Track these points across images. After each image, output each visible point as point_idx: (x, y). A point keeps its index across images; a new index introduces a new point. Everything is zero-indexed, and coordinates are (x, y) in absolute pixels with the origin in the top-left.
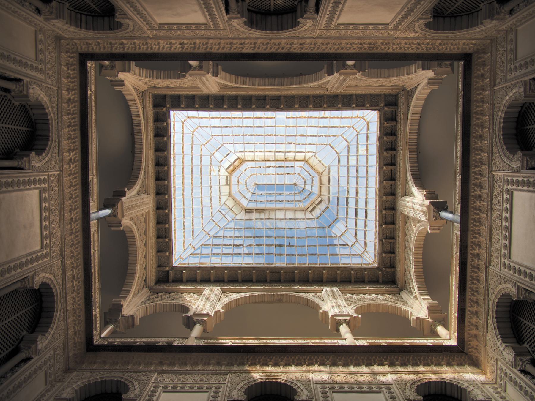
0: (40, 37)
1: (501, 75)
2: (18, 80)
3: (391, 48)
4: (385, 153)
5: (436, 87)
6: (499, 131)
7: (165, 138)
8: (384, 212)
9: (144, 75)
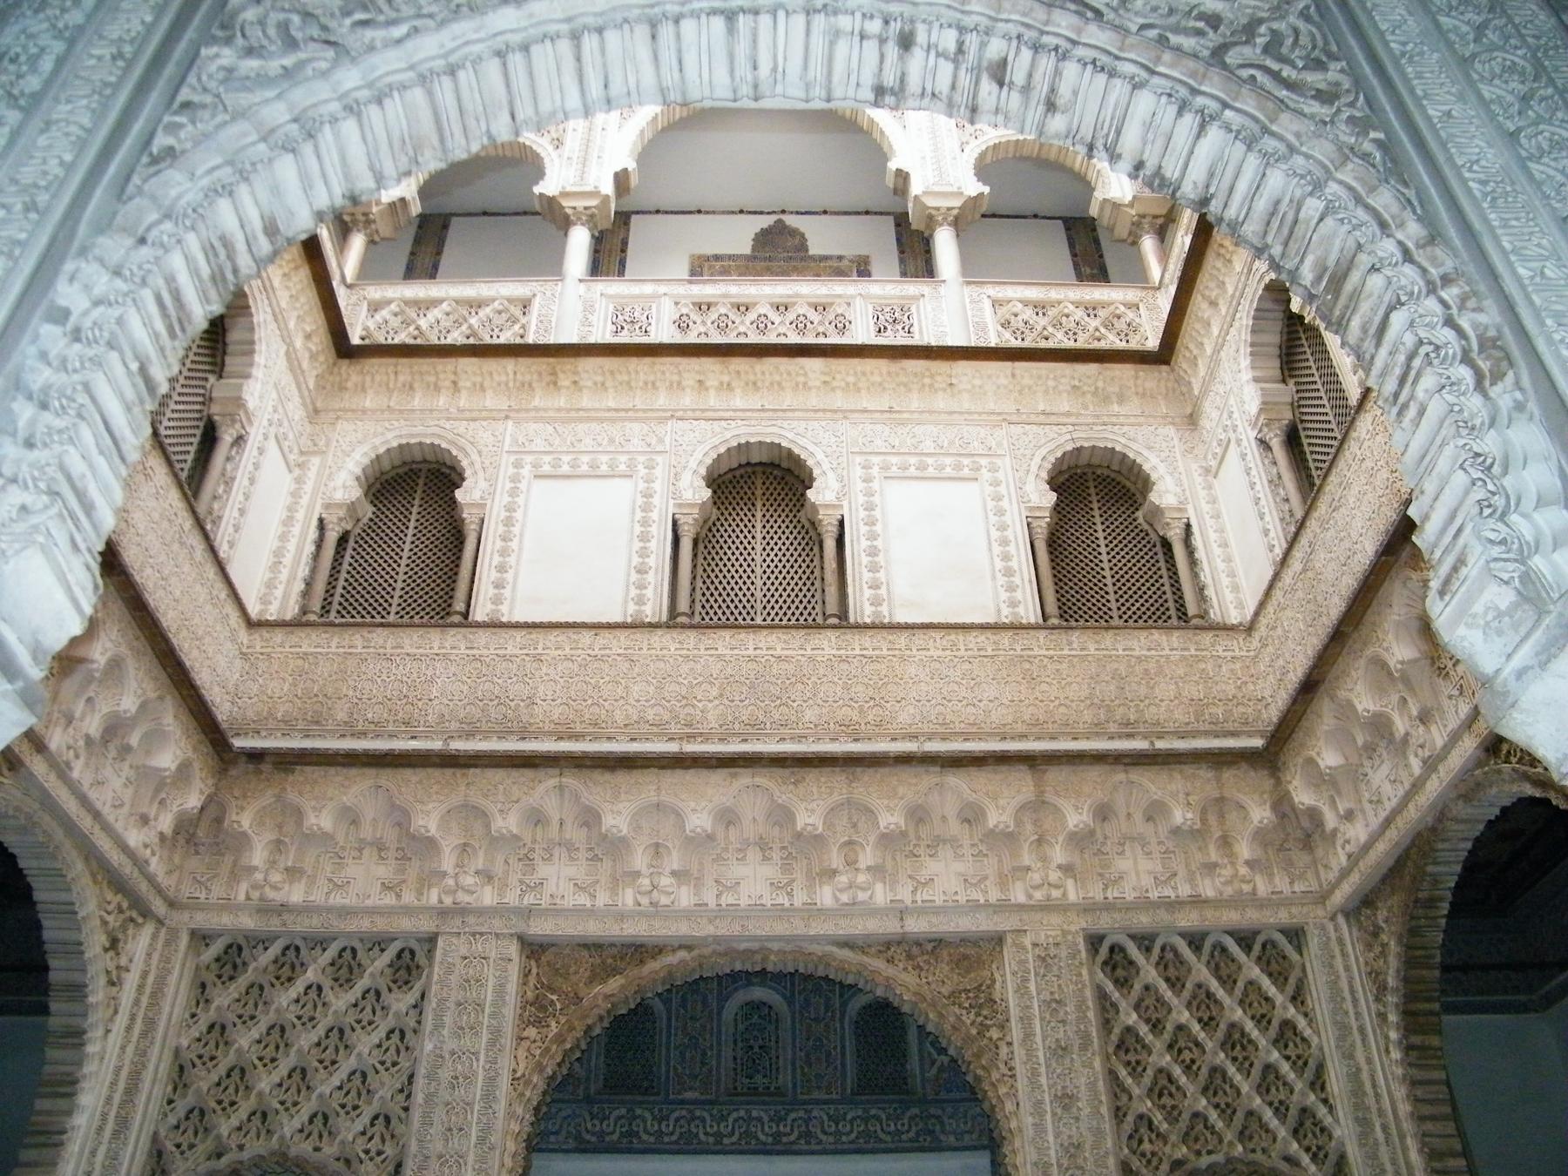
0: (1214, 463)
2: (1264, 444)
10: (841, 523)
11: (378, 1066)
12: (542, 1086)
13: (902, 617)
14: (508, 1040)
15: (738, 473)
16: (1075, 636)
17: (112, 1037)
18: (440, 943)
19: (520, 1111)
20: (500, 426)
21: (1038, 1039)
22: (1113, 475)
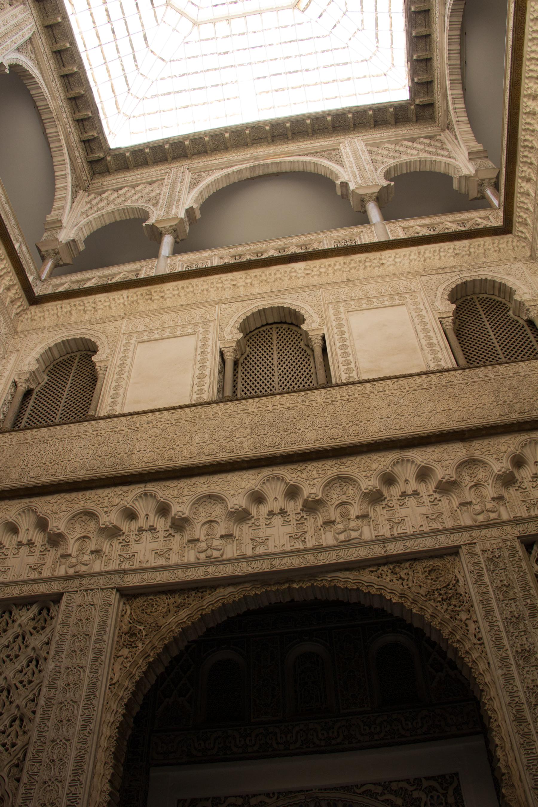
3: (125, 297)
4: (83, 92)
5: (49, 218)
7: (415, 57)
9: (443, 165)
10: (323, 338)
13: (365, 377)
14: (106, 658)
15: (261, 330)
16: (479, 371)
18: (64, 598)
19: (114, 707)
20: (119, 323)
21: (497, 613)
22: (490, 296)
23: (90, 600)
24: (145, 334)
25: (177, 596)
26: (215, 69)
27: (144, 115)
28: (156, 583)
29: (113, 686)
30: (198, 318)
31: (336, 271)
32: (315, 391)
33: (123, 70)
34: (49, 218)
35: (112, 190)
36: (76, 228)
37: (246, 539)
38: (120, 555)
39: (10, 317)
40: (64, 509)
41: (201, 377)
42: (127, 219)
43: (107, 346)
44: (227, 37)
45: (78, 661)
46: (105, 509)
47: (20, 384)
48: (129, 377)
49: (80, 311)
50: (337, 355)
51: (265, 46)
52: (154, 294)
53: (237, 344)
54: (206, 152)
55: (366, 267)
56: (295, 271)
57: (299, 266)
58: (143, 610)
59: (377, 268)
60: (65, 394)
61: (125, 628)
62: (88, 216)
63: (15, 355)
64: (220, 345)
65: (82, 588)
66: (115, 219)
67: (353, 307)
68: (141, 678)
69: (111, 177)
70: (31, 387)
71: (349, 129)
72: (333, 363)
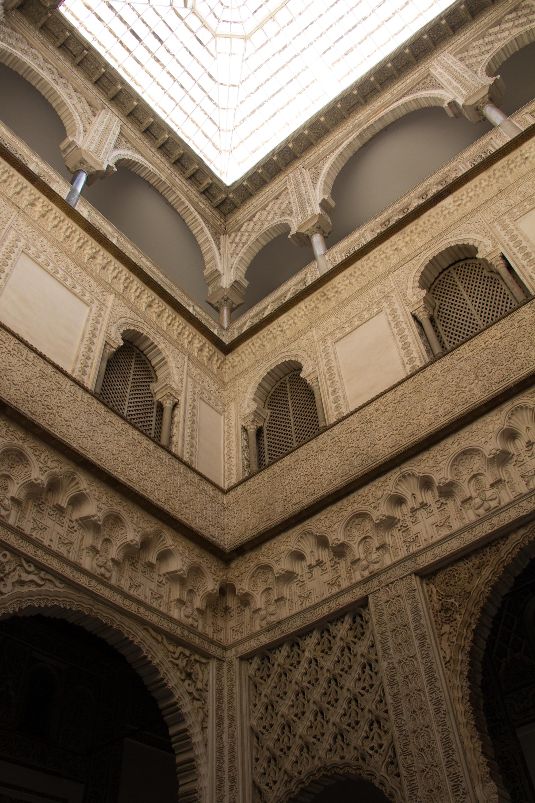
1: (195, 371)
3: (304, 308)
4: (182, 152)
5: (206, 273)
6: (148, 333)
8: (120, 87)
10: (503, 257)
11: (363, 692)
12: (467, 659)
14: (431, 640)
15: (440, 278)
17: (209, 731)
18: (371, 600)
19: (457, 682)
20: (309, 334)
23: (394, 592)
24: (337, 332)
25: (473, 558)
26: (283, 67)
27: (242, 142)
28: (448, 553)
29: (448, 664)
30: (377, 295)
31: (484, 188)
32: (518, 310)
33: (206, 114)
34: (206, 273)
35: (247, 221)
36: (232, 270)
37: (517, 478)
38: (404, 542)
39: (214, 374)
40: (335, 520)
41: (406, 347)
42: (272, 240)
43: (308, 359)
44: (279, 32)
45: (407, 652)
46: (373, 505)
47: (249, 427)
48: (340, 377)
49: (270, 339)
50: (523, 266)
51: (316, 20)
52: (328, 293)
53: (424, 302)
54: (312, 144)
55: (511, 169)
56: (446, 208)
57: (448, 202)
58: (447, 583)
59: (523, 165)
60: (291, 418)
61: (437, 607)
62: (237, 254)
63: (233, 404)
64: (409, 310)
65: (383, 585)
66: (262, 244)
67: (518, 213)
68: (472, 647)
69: (241, 210)
70: (259, 425)
71: (430, 50)
72: (524, 276)
